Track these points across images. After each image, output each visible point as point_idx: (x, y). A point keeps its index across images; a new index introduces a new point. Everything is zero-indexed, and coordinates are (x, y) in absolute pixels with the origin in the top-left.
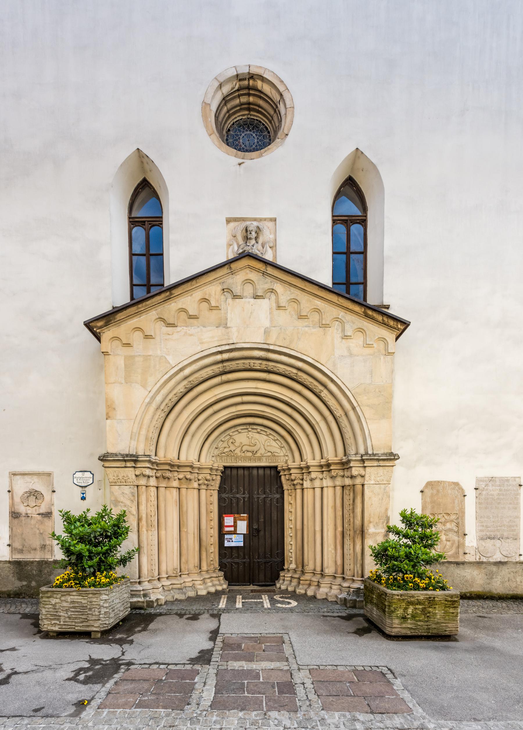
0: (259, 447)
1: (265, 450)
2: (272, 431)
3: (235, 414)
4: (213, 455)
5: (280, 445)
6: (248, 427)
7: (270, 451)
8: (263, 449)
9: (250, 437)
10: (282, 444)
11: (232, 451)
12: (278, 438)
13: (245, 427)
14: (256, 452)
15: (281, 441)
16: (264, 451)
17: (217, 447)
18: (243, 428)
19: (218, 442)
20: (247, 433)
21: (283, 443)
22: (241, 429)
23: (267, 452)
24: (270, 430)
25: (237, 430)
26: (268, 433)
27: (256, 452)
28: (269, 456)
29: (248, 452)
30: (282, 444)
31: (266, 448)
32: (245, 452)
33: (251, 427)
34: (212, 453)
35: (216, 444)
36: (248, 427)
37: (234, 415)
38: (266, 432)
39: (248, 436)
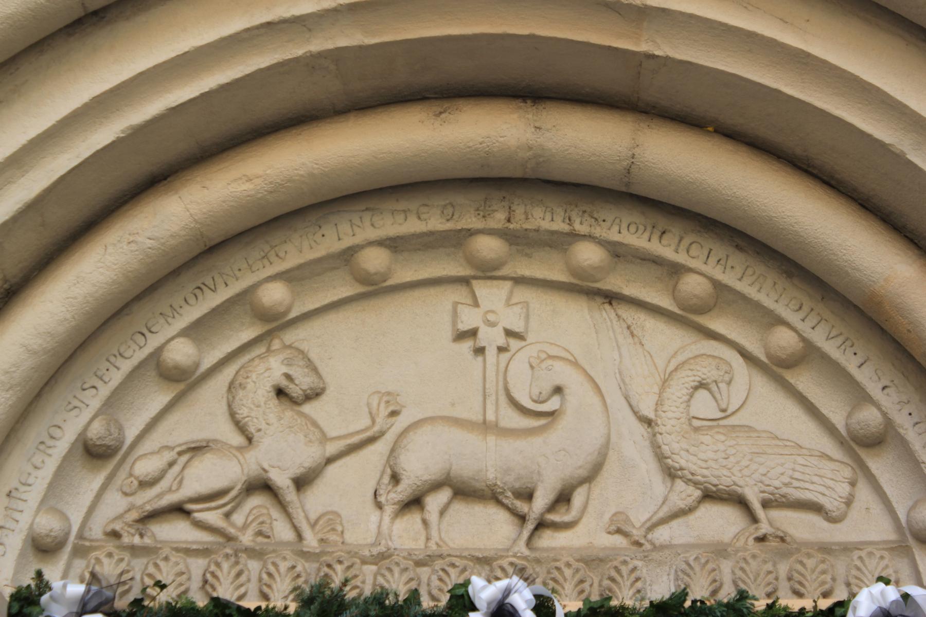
0: (593, 437)
1: (671, 474)
2: (738, 260)
3: (318, 44)
4: (48, 524)
5: (838, 418)
6: (471, 221)
7: (725, 479)
8: (648, 467)
9: (491, 337)
10: (860, 396)
11: (282, 480)
12: (819, 337)
13: (435, 222)
14: (563, 498)
15: (851, 364)
16: (658, 485)
17: (97, 431)
18: (412, 226)
19: (116, 378)
20: (456, 294)
21: (874, 389)
22: (394, 244)
23: (684, 494)
24: (720, 250)
25: (348, 256)
26: (694, 285)
27: (563, 498)
28: (720, 550)
29: (463, 511)
30: (860, 396)
31: (672, 443)
32: (435, 502)
33: (498, 219)
34: (34, 496)
35: (95, 401)
36: (471, 221)
37: (312, 62)
38: (675, 270)
39: (469, 319)
